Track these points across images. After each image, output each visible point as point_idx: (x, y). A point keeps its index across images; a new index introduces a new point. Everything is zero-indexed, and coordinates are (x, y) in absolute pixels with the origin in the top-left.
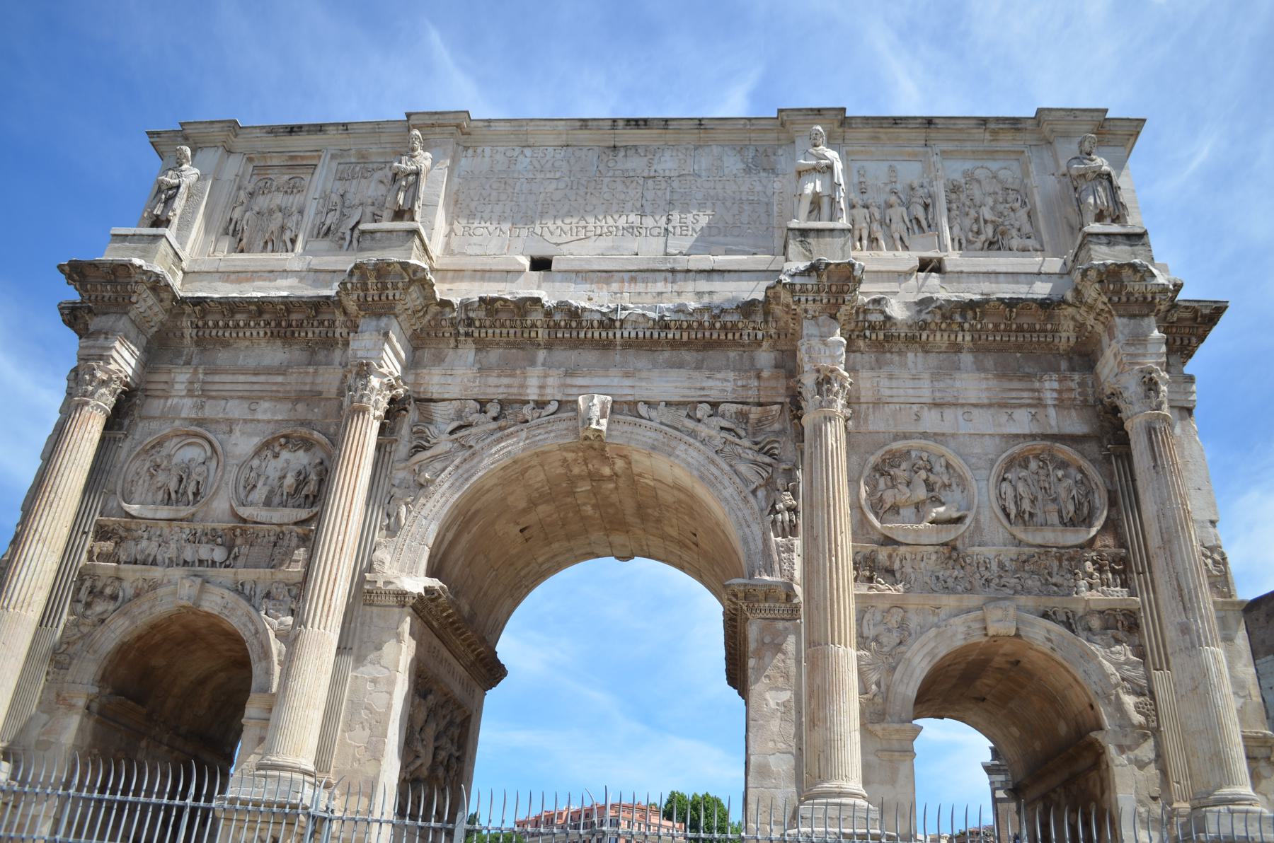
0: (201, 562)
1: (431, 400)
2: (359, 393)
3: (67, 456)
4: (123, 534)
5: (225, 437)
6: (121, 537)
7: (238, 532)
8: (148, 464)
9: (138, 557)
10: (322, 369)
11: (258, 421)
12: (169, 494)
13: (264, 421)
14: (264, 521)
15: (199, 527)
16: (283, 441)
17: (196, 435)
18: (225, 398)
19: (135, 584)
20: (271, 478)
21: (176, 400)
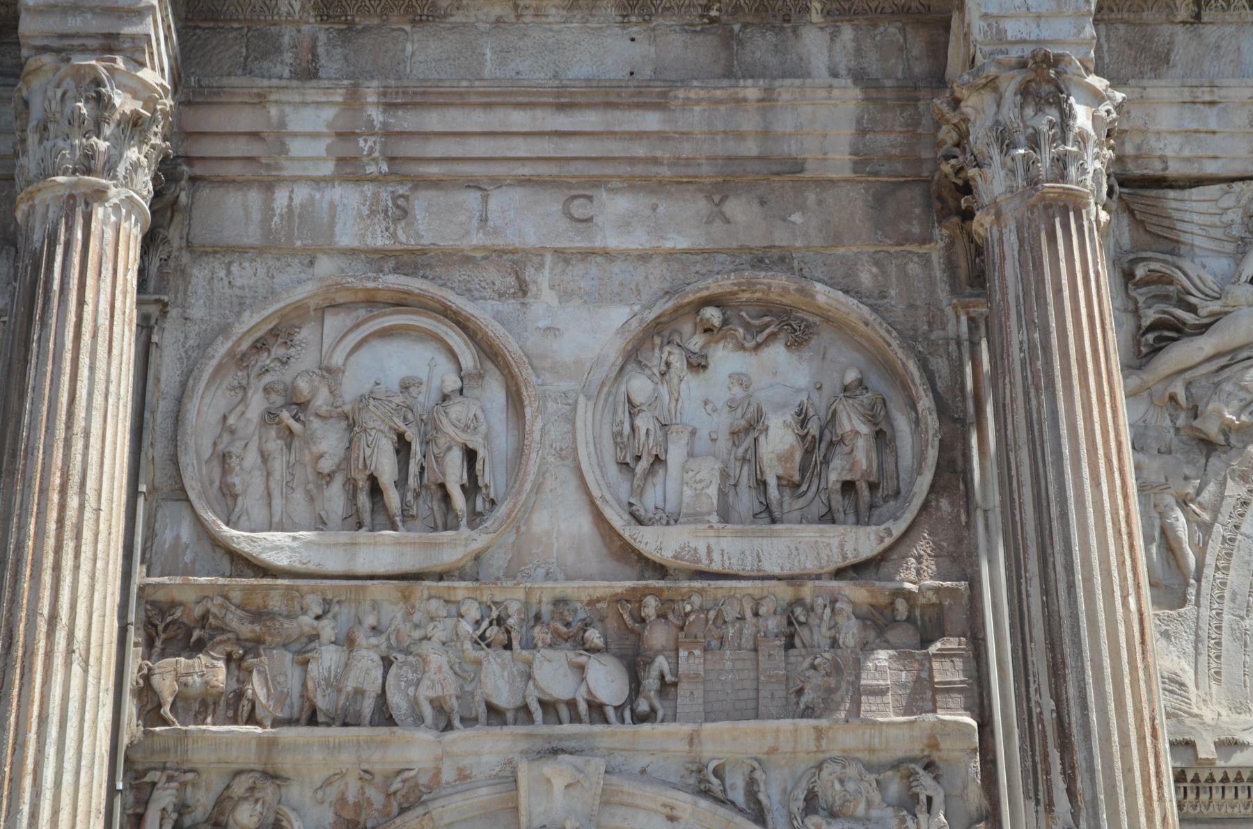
0: (549, 707)
1: (1161, 182)
2: (1047, 154)
3: (84, 372)
4: (247, 630)
5: (509, 307)
6: (238, 640)
7: (651, 607)
8: (257, 404)
9: (321, 703)
10: (786, 90)
11: (606, 254)
12: (375, 490)
13: (626, 255)
14: (736, 568)
15: (513, 599)
16: (712, 315)
17: (401, 302)
18: (473, 184)
19: (333, 792)
20: (703, 434)
21: (302, 193)
